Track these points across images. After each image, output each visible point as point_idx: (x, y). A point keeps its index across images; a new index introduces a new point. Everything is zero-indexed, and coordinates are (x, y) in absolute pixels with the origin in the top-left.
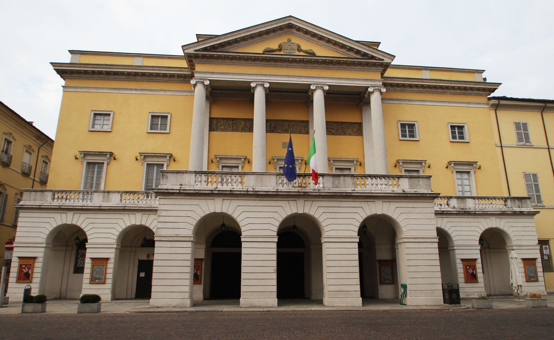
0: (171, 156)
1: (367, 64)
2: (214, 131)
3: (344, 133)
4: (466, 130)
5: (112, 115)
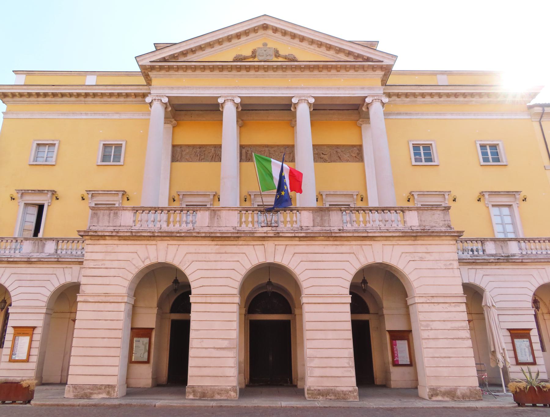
0: (124, 193)
2: (177, 161)
3: (340, 159)
4: (501, 150)
5: (57, 145)
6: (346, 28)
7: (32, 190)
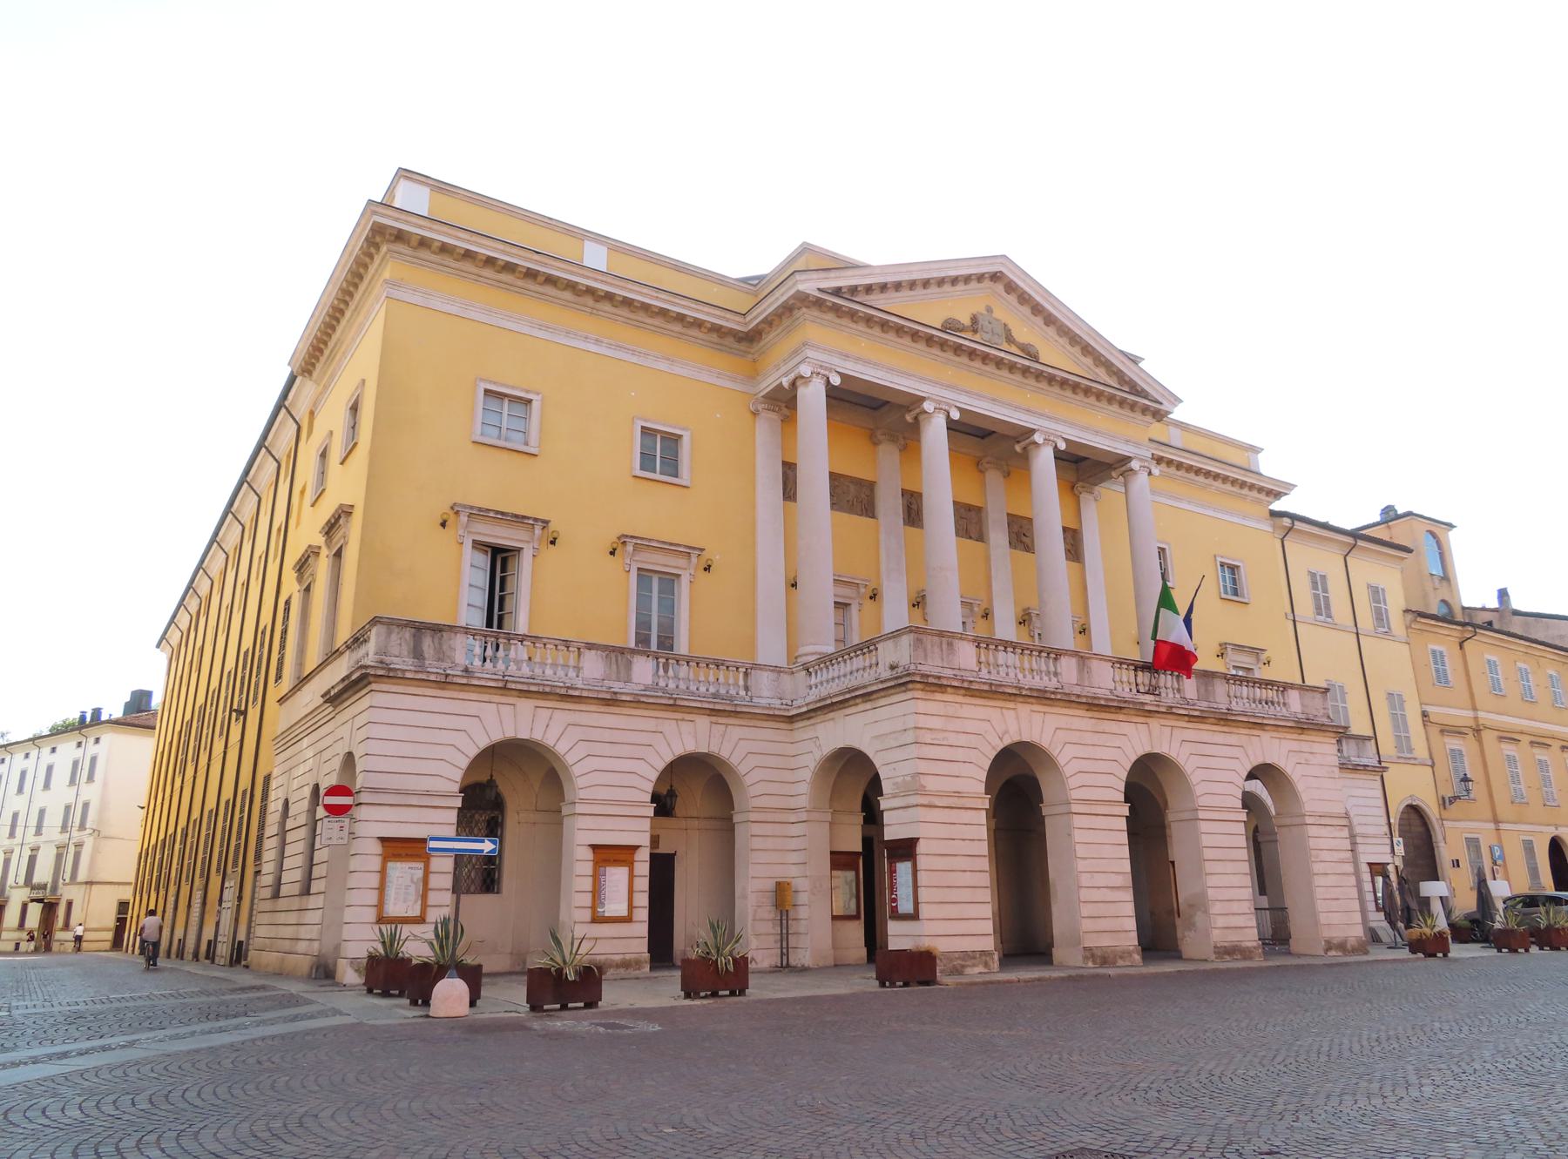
1: (1133, 406)
4: (1245, 575)
6: (1116, 326)
7: (497, 512)
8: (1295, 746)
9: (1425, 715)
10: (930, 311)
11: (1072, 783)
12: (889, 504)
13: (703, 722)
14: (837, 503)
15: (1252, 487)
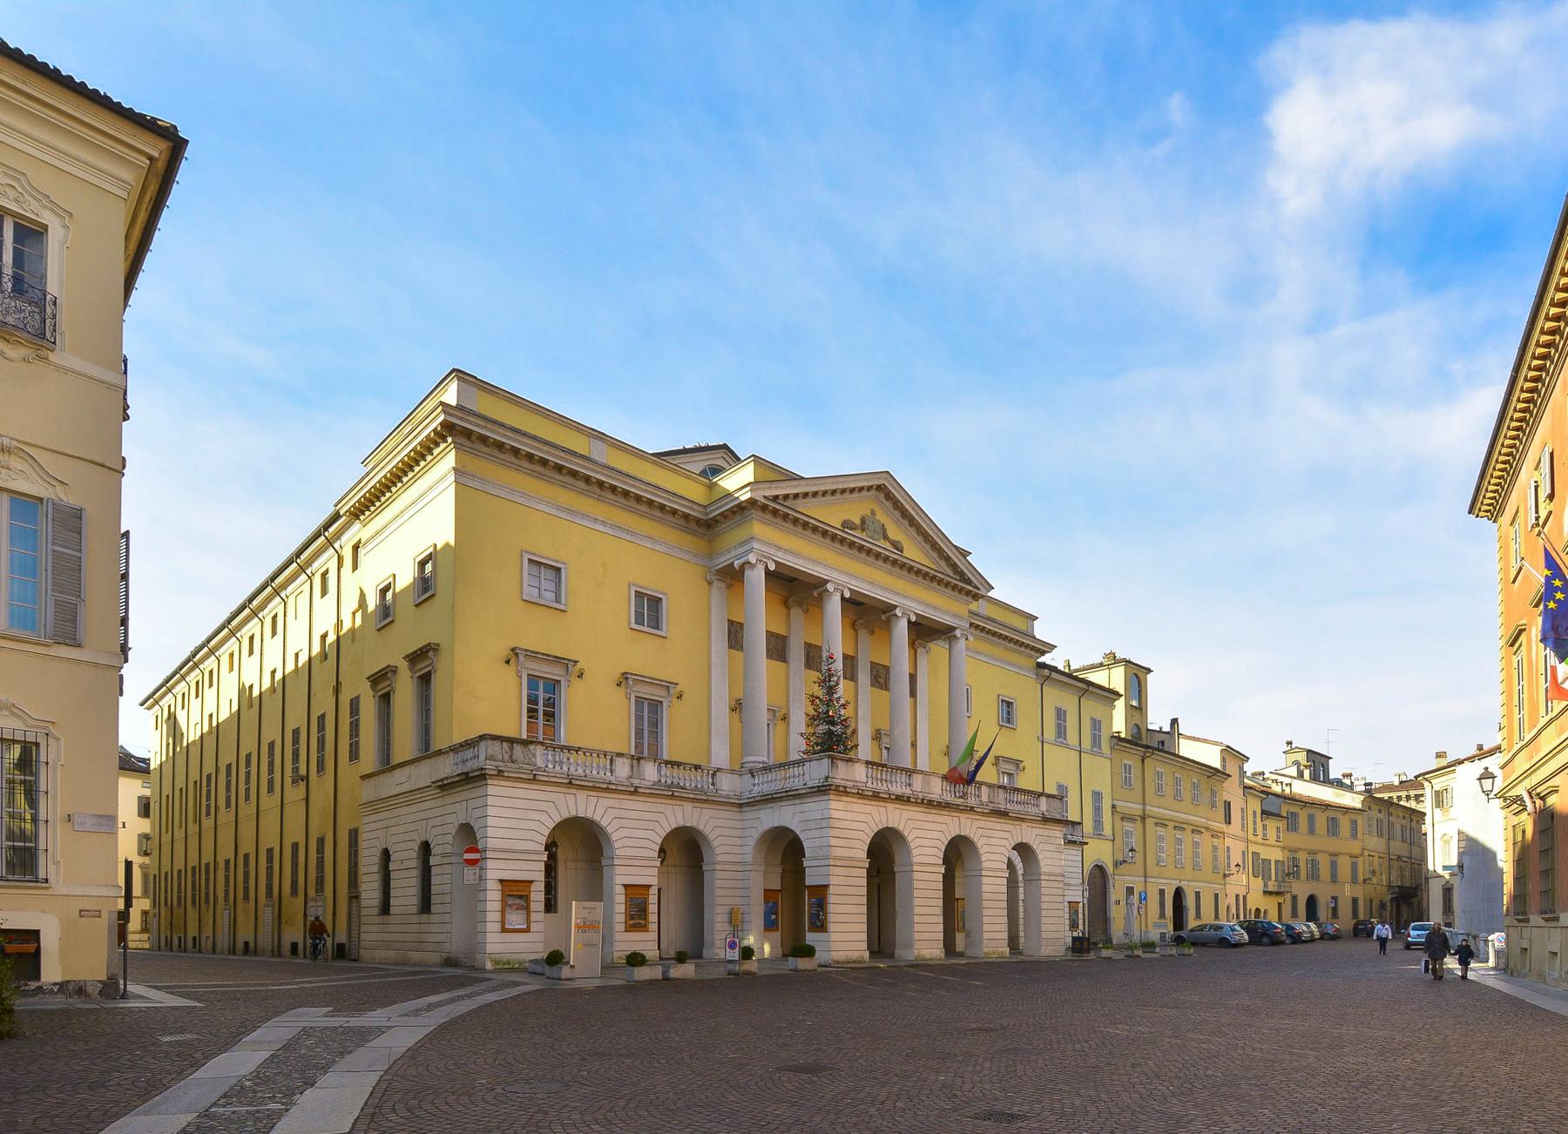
1: (961, 590)
8: (1041, 832)
9: (1114, 807)
10: (832, 515)
11: (915, 852)
12: (797, 653)
13: (688, 806)
14: (770, 655)
15: (1027, 646)
